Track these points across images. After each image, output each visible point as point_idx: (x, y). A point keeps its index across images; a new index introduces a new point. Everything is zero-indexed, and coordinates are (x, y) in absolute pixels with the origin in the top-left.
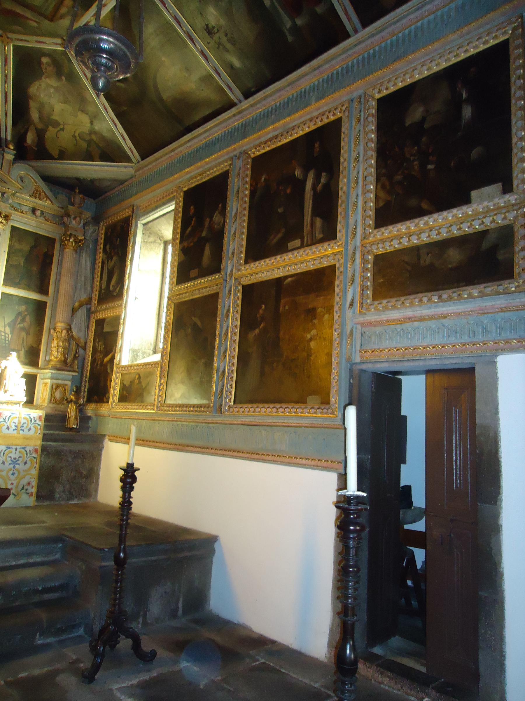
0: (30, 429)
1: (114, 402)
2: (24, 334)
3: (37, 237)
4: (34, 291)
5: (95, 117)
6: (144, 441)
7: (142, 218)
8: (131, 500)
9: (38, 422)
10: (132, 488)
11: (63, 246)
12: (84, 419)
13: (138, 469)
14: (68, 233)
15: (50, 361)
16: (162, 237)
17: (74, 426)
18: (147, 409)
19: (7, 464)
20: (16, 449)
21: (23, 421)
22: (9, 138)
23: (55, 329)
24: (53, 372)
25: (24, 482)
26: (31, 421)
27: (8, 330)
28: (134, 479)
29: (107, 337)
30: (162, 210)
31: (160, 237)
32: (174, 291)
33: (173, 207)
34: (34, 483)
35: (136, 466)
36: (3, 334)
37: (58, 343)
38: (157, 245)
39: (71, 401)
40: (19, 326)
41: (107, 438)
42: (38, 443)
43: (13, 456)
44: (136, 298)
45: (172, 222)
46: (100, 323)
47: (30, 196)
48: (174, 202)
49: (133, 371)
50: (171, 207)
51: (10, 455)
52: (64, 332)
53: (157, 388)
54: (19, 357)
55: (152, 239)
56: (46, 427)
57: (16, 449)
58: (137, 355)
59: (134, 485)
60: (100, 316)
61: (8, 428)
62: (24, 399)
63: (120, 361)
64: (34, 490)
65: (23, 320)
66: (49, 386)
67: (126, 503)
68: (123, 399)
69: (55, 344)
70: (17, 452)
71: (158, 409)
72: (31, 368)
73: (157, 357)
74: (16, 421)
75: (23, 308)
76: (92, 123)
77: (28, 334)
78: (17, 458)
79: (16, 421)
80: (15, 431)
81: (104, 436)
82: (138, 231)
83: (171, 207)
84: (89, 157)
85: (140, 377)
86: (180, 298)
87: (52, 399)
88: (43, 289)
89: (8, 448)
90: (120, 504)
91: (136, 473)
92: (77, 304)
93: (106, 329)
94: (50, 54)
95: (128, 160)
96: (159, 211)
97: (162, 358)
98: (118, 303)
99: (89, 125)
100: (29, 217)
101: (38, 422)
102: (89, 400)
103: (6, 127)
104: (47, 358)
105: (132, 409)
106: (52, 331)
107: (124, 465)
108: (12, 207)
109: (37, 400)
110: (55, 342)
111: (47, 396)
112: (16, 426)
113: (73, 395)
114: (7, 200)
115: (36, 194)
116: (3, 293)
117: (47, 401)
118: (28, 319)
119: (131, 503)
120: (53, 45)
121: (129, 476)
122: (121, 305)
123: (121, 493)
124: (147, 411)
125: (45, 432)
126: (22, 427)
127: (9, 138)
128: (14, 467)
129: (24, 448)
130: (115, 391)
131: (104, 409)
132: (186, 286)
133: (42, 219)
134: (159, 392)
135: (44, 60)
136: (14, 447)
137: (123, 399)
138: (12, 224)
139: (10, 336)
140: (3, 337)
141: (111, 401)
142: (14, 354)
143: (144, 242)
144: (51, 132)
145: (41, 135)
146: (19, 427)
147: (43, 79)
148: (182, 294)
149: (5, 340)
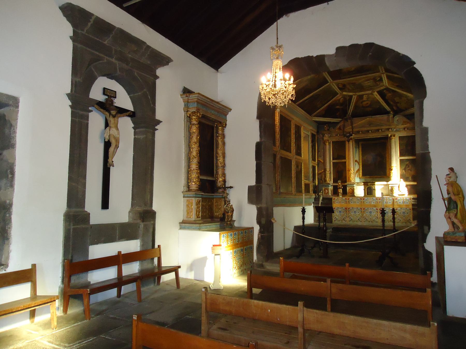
4: (411, 156)
25: (408, 219)
27: (404, 171)
42: (411, 207)
43: (403, 211)
65: (408, 167)
75: (408, 163)
77: (411, 171)
115: (404, 123)
118: (410, 166)
135: (385, 91)
144: (399, 105)
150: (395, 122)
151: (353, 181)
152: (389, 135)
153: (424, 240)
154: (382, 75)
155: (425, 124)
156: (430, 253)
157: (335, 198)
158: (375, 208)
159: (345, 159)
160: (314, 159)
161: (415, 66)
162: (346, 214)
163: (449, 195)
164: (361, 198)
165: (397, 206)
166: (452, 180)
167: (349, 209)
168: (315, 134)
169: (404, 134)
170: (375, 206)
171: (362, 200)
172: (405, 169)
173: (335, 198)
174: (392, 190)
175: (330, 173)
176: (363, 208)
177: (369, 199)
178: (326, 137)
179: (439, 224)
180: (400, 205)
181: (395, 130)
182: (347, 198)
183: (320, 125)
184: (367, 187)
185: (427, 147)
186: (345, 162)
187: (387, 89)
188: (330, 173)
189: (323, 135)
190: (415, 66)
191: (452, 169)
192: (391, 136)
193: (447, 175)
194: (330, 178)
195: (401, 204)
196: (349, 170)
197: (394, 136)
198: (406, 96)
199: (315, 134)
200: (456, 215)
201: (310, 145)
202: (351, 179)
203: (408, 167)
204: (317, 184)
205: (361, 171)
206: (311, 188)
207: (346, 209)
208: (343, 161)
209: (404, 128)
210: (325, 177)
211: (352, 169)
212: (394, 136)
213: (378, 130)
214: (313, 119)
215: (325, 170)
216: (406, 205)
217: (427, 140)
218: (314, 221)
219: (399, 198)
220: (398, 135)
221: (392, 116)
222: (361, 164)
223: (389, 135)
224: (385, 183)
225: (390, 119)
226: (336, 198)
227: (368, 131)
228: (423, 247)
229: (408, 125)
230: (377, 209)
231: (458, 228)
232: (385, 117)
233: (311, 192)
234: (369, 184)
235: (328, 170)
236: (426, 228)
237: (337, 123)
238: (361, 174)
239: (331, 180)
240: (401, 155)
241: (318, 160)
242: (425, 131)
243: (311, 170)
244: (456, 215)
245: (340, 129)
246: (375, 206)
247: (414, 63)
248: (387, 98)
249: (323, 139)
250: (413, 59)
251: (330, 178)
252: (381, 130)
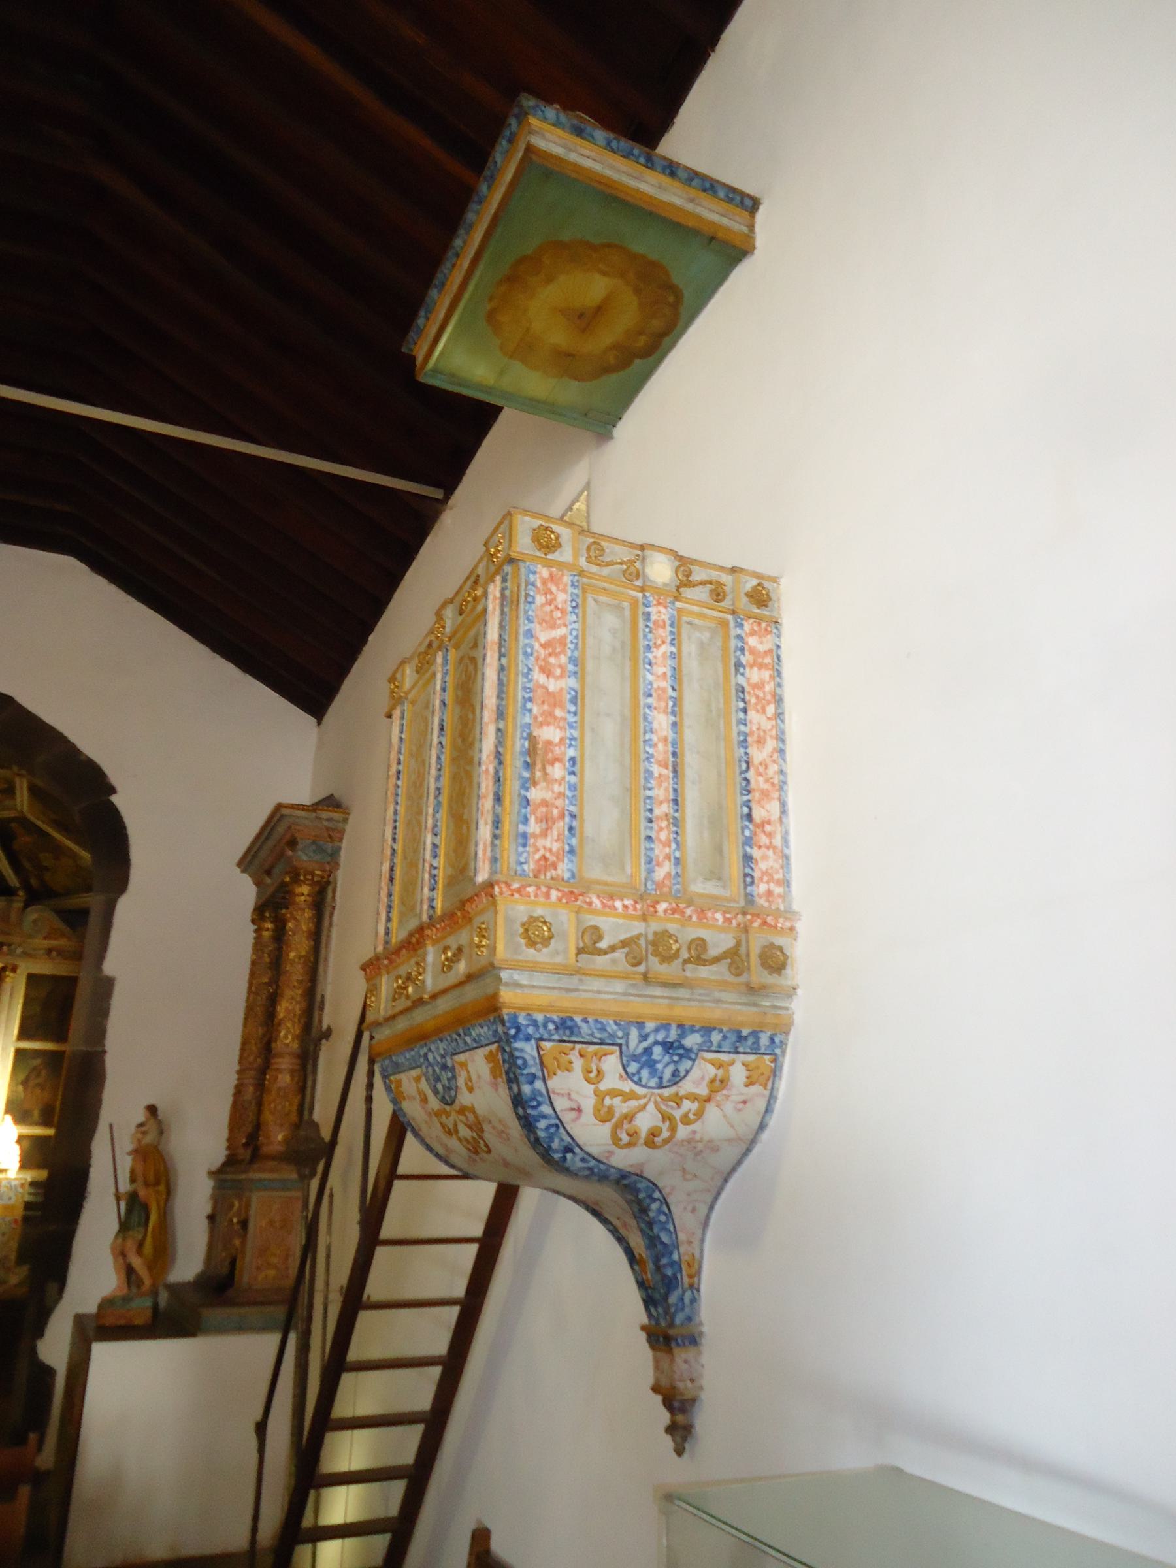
2: (38, 1091)
3: (54, 979)
27: (20, 1088)
47: (45, 938)
65: (38, 1075)
77: (43, 1090)
94: (14, 819)
118: (44, 1073)
127: (18, 885)
135: (13, 825)
150: (27, 925)
153: (39, 1332)
154: (17, 780)
155: (110, 967)
156: (50, 1372)
161: (114, 799)
163: (134, 1186)
166: (148, 1139)
169: (44, 968)
172: (25, 1083)
179: (94, 1272)
181: (19, 950)
185: (98, 1033)
187: (22, 820)
190: (114, 799)
191: (152, 1110)
193: (141, 1125)
197: (14, 970)
198: (74, 856)
200: (140, 1245)
203: (38, 1075)
209: (49, 951)
212: (14, 970)
217: (105, 1013)
220: (26, 967)
221: (18, 904)
225: (14, 916)
228: (33, 1351)
229: (61, 942)
231: (140, 1283)
236: (52, 1287)
240: (24, 1034)
242: (105, 987)
244: (140, 1245)
247: (113, 790)
250: (114, 778)
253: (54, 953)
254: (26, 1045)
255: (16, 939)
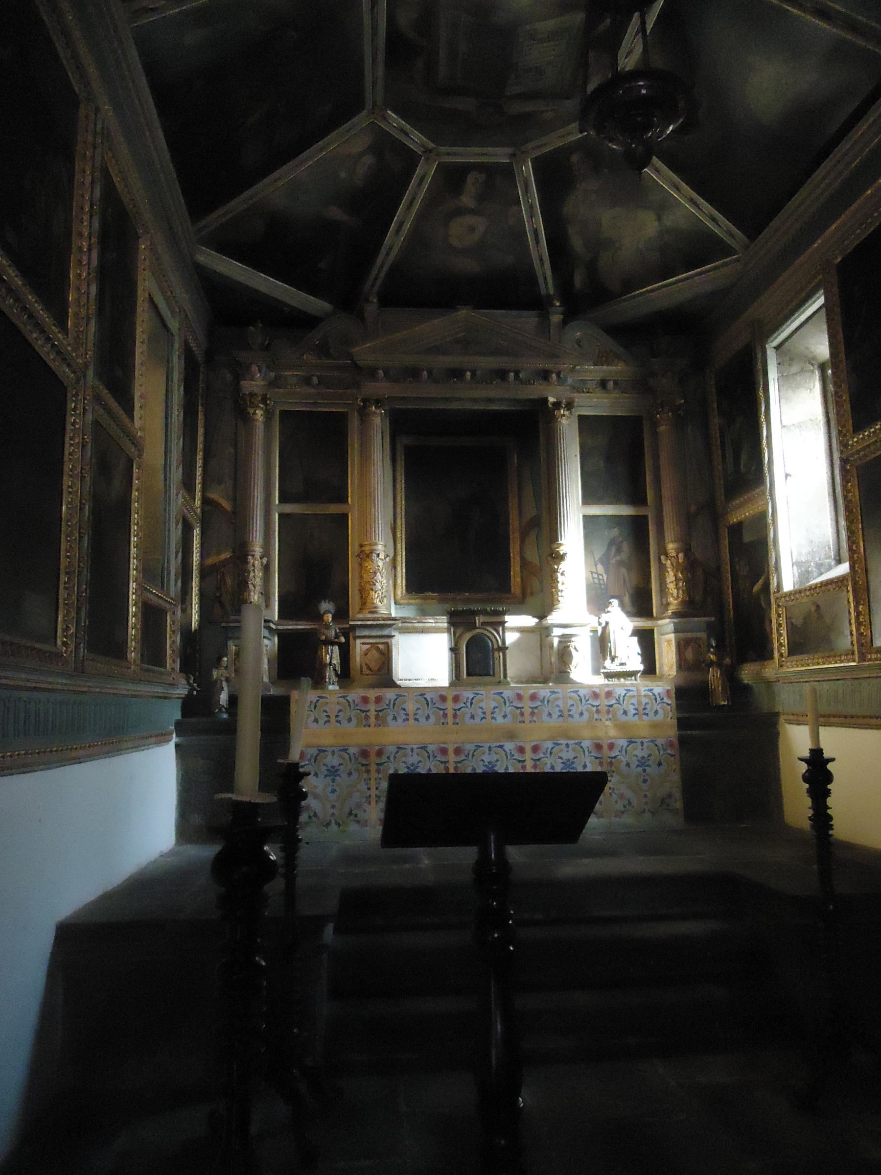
0: (656, 712)
1: (781, 655)
2: (624, 571)
3: (613, 422)
5: (663, 206)
6: (846, 717)
7: (772, 338)
8: (829, 811)
9: (666, 700)
10: (828, 793)
11: (655, 425)
12: (739, 691)
13: (833, 760)
14: (659, 402)
15: (668, 604)
16: (814, 358)
17: (723, 703)
18: (842, 662)
19: (633, 766)
20: (642, 743)
21: (644, 700)
22: (552, 292)
23: (666, 555)
24: (676, 620)
26: (656, 699)
27: (600, 569)
28: (828, 777)
29: (752, 549)
30: (803, 312)
31: (811, 360)
32: (852, 445)
33: (820, 301)
34: (678, 795)
35: (827, 755)
36: (595, 576)
37: (675, 576)
38: (807, 374)
39: (711, 664)
40: (613, 561)
41: (782, 719)
42: (672, 732)
43: (640, 753)
44: (787, 475)
45: (825, 327)
46: (737, 530)
48: (822, 292)
49: (804, 601)
50: (819, 301)
51: (635, 753)
52: (681, 555)
53: (853, 621)
54: (622, 605)
55: (795, 369)
56: (679, 707)
57: (642, 743)
58: (808, 572)
59: (829, 787)
60: (734, 519)
61: (625, 713)
62: (641, 667)
63: (779, 586)
64: (679, 805)
65: (619, 551)
66: (673, 643)
67: (822, 818)
68: (796, 648)
69: (670, 577)
70: (644, 747)
71: (862, 658)
72: (643, 619)
73: (844, 568)
74: (634, 701)
75: (615, 532)
76: (659, 218)
77: (629, 570)
78: (646, 756)
79: (634, 701)
80: (636, 717)
81: (777, 714)
82: (769, 362)
83: (819, 301)
84: (666, 272)
85: (818, 606)
86: (865, 456)
87: (682, 663)
88: (637, 497)
89: (631, 742)
90: (810, 818)
91: (830, 766)
92: (693, 508)
93: (747, 538)
94: (578, 146)
95: (727, 251)
96: (799, 316)
97: (852, 567)
98: (758, 490)
99: (656, 224)
100: (599, 395)
101: (666, 700)
102: (742, 659)
103: (545, 278)
104: (664, 603)
105: (813, 664)
106: (663, 557)
107: (806, 754)
108: (574, 388)
109: (660, 668)
110: (671, 573)
111: (674, 660)
112: (636, 709)
113: (712, 654)
114: (565, 380)
116: (584, 516)
117: (675, 667)
119: (830, 818)
120: (573, 134)
121: (818, 770)
122: (764, 493)
123: (808, 802)
124: (842, 665)
125: (680, 715)
126: (645, 709)
127: (552, 292)
128: (644, 771)
129: (652, 741)
130: (780, 638)
131: (770, 671)
132: (872, 430)
133: (616, 394)
134: (858, 629)
136: (639, 741)
137: (796, 648)
138: (578, 413)
139: (605, 577)
140: (596, 581)
141: (776, 655)
142: (615, 602)
143: (784, 378)
145: (592, 268)
146: (641, 709)
147: (578, 186)
148: (868, 446)
149: (600, 584)
151: (383, 611)
152: (551, 399)
157: (303, 698)
158: (509, 746)
159: (342, 498)
160: (188, 485)
162: (363, 787)
164: (440, 695)
165: (612, 732)
167: (380, 753)
168: (200, 357)
170: (511, 736)
171: (450, 705)
172: (605, 561)
173: (303, 698)
174: (564, 654)
175: (267, 568)
176: (451, 749)
177: (485, 696)
178: (255, 383)
180: (622, 727)
182: (372, 694)
183: (229, 316)
184: (467, 636)
186: (345, 517)
188: (267, 568)
189: (240, 372)
192: (557, 405)
194: (266, 595)
195: (631, 718)
196: (366, 555)
197: (569, 406)
199: (200, 357)
201: (178, 394)
202: (376, 598)
204: (194, 624)
205: (401, 570)
206: (173, 641)
207: (365, 753)
208: (334, 509)
209: (603, 384)
210: (243, 585)
211: (380, 548)
212: (569, 406)
213: (501, 374)
214: (201, 258)
215: (242, 553)
216: (654, 726)
218: (184, 832)
219: (621, 691)
221: (556, 318)
222: (401, 534)
223: (551, 399)
224: (529, 621)
226: (312, 695)
227: (456, 373)
229: (616, 369)
230: (521, 750)
232: (528, 320)
233: (172, 662)
234: (479, 620)
235: (258, 550)
237: (308, 322)
238: (401, 581)
239: (268, 605)
240: (589, 497)
241: (205, 501)
243: (175, 533)
245: (323, 350)
246: (511, 736)
248: (568, 208)
249: (237, 388)
251: (266, 595)
252: (517, 373)
253: (611, 384)
254: (596, 510)
255: (566, 366)
